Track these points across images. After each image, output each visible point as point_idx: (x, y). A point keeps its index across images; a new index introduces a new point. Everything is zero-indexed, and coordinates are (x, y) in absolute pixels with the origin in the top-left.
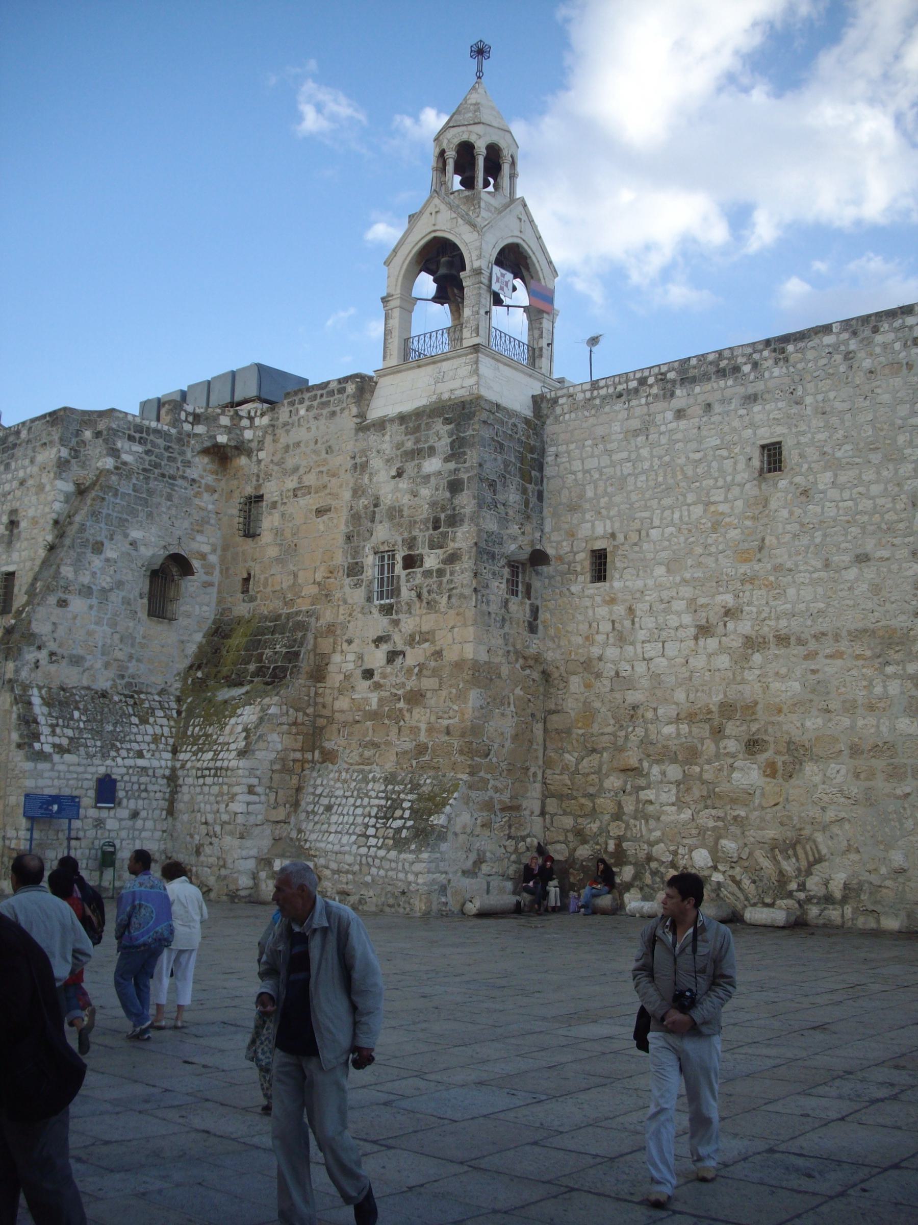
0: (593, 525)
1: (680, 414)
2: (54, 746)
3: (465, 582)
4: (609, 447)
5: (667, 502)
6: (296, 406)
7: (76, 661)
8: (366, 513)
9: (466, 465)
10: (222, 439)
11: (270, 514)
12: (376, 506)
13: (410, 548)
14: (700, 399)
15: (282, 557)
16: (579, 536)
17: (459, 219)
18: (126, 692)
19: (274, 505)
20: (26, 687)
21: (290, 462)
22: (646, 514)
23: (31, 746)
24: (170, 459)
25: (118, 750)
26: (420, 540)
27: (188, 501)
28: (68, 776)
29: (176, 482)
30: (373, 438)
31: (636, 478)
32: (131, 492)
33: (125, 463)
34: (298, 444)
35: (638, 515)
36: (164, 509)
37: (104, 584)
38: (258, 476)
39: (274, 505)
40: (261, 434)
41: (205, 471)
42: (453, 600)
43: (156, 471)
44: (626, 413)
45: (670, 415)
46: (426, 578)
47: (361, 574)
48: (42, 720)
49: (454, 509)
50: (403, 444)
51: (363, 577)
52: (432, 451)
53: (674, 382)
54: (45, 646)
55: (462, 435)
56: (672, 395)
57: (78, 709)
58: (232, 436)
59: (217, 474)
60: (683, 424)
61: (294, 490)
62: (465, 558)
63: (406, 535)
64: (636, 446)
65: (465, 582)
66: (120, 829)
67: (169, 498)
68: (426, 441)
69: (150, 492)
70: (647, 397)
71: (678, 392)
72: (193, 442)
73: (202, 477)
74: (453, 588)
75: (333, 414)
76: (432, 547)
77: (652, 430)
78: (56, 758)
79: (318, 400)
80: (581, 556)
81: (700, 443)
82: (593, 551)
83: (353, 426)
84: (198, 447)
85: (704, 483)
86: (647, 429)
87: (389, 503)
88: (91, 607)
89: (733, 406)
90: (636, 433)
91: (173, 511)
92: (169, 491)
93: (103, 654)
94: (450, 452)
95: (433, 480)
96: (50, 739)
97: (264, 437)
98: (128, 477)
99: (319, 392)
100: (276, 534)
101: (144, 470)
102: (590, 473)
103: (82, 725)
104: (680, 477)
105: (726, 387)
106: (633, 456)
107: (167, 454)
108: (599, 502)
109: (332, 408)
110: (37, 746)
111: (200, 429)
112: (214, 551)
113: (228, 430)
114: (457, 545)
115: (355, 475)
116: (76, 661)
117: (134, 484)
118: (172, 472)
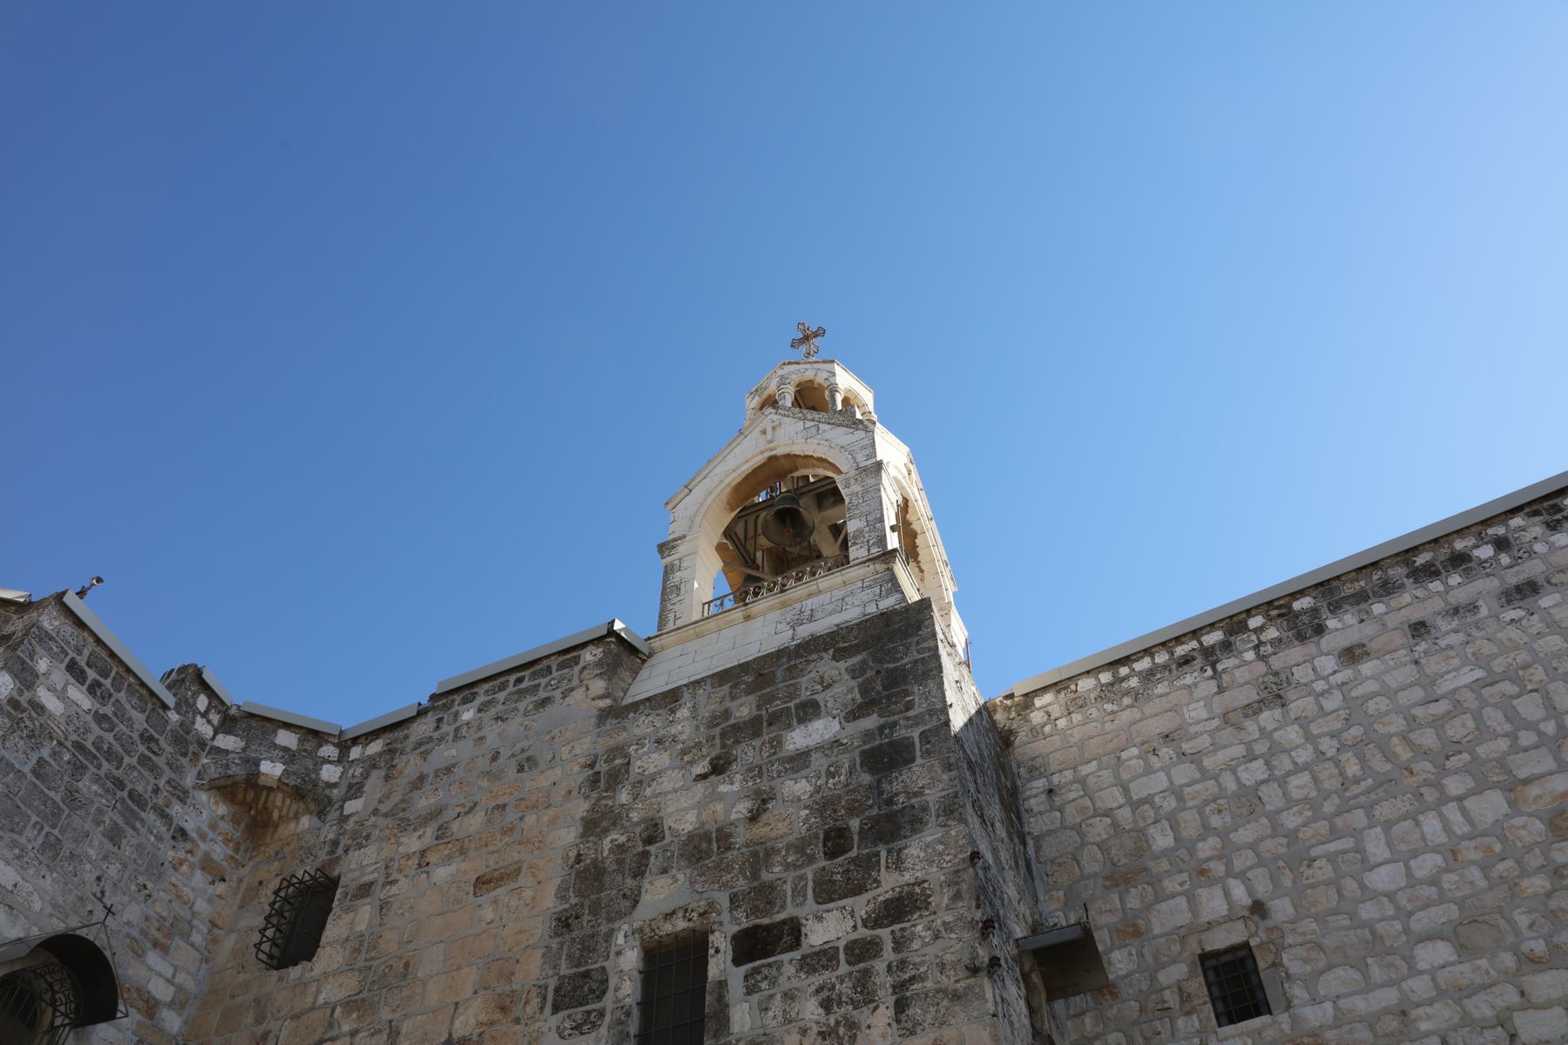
0: (1191, 899)
1: (1352, 655)
3: (949, 958)
4: (1186, 747)
5: (1384, 811)
6: (456, 708)
8: (620, 862)
9: (911, 713)
10: (271, 769)
11: (347, 910)
12: (650, 840)
13: (755, 911)
14: (1392, 620)
15: (365, 994)
16: (1157, 931)
17: (821, 425)
19: (365, 890)
21: (423, 802)
22: (1345, 843)
24: (143, 760)
26: (788, 888)
27: (156, 868)
29: (143, 814)
30: (643, 725)
31: (1282, 782)
32: (26, 769)
33: (39, 708)
34: (448, 770)
35: (1314, 852)
36: (92, 853)
38: (335, 843)
39: (365, 890)
40: (359, 771)
41: (213, 827)
42: (915, 1011)
43: (105, 765)
44: (1213, 683)
45: (1327, 664)
46: (812, 970)
47: (599, 998)
49: (890, 802)
50: (727, 714)
51: (608, 1001)
52: (809, 711)
53: (1314, 611)
55: (891, 666)
56: (1320, 630)
58: (295, 767)
59: (237, 850)
60: (1367, 668)
61: (423, 853)
62: (941, 899)
63: (742, 884)
64: (1262, 730)
65: (949, 958)
67: (114, 835)
68: (791, 697)
69: (71, 796)
70: (1257, 647)
71: (1332, 623)
72: (206, 761)
73: (203, 837)
74: (913, 979)
75: (545, 702)
76: (827, 892)
77: (1290, 695)
79: (511, 689)
80: (1179, 971)
81: (1433, 683)
82: (1205, 957)
83: (596, 713)
84: (213, 772)
85: (1481, 750)
86: (1280, 697)
87: (689, 827)
89: (1484, 612)
90: (1251, 710)
91: (113, 870)
92: (120, 821)
94: (859, 699)
95: (819, 762)
97: (365, 775)
98: (35, 737)
99: (512, 678)
100: (357, 950)
101: (79, 746)
102: (1153, 805)
104: (1405, 754)
105: (1449, 588)
106: (1261, 748)
107: (142, 749)
108: (1192, 853)
109: (542, 694)
111: (228, 742)
112: (178, 1004)
113: (288, 756)
114: (908, 877)
115: (594, 795)
117: (41, 759)
118: (140, 789)
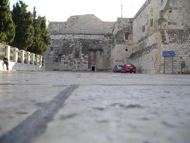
2: (169, 41)
7: (175, 24)
18: (188, 30)
20: (163, 30)
23: (164, 41)
25: (185, 42)
28: (173, 48)
37: (180, 7)
48: (167, 36)
54: (167, 21)
57: (175, 34)
66: (187, 59)
78: (170, 44)
88: (177, 12)
93: (181, 22)
96: (168, 40)
103: (176, 37)
110: (165, 41)
116: (175, 24)
